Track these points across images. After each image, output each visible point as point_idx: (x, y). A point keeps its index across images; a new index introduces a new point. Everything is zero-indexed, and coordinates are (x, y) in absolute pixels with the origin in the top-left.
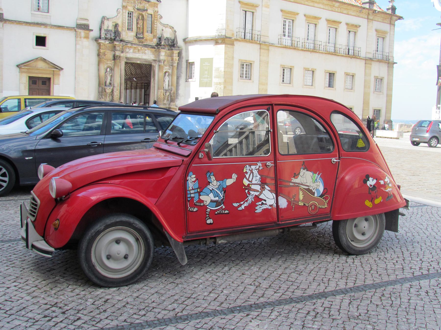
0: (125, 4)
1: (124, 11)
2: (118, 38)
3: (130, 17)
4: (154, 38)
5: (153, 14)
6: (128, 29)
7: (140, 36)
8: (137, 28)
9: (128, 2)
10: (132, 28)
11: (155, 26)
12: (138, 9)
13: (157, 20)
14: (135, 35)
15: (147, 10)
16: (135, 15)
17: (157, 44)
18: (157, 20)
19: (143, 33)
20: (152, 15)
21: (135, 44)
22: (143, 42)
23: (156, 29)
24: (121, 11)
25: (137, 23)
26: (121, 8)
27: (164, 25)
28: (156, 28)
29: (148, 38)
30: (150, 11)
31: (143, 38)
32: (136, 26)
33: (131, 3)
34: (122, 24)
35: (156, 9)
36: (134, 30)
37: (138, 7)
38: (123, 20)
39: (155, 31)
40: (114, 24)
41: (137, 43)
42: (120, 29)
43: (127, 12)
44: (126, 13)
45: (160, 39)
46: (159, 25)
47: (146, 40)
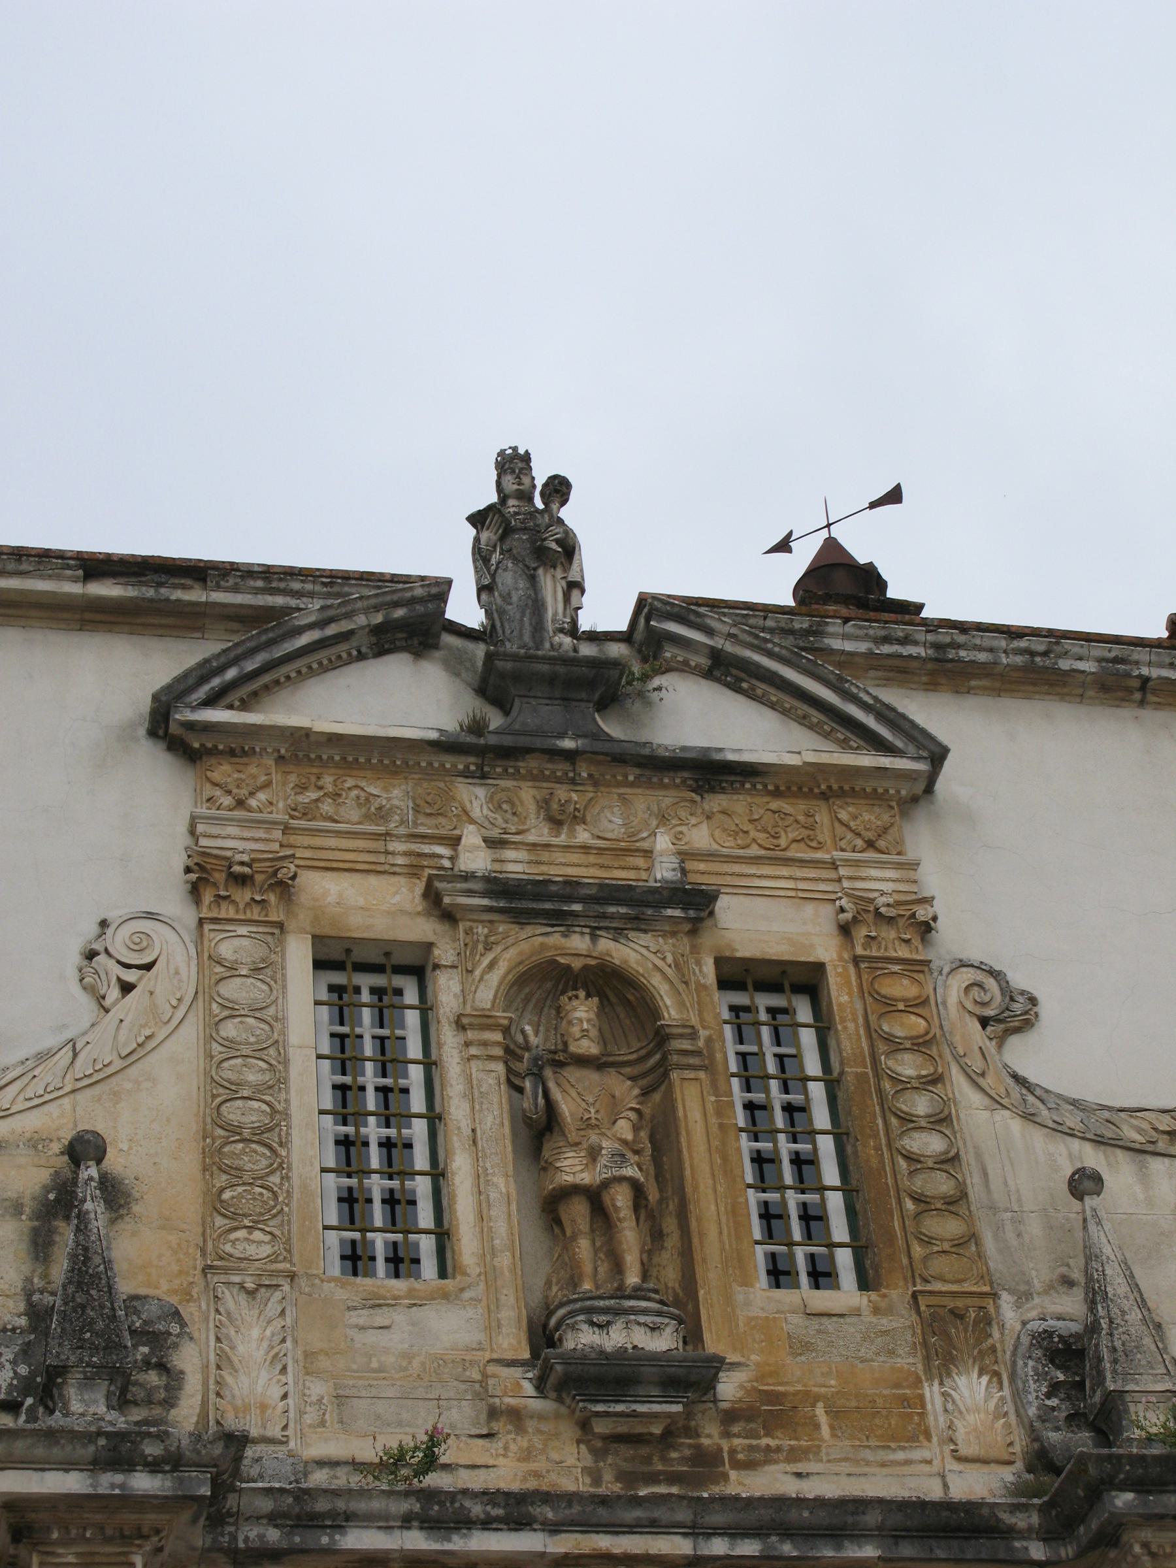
0: (235, 841)
1: (236, 945)
2: (86, 1405)
3: (389, 1059)
4: (941, 1358)
5: (824, 948)
6: (355, 1259)
7: (616, 1338)
8: (552, 1206)
9: (307, 813)
10: (443, 1235)
11: (931, 1144)
12: (518, 900)
13: (921, 1044)
14: (513, 1341)
15: (694, 903)
16: (472, 982)
17: (1042, 1460)
18: (921, 1044)
19: (686, 1313)
20: (806, 980)
21: (515, 1510)
22: (707, 1464)
23: (956, 1201)
24: (174, 950)
25: (539, 1132)
26: (175, 904)
27: (1103, 1127)
28: (940, 1185)
29: (796, 1375)
30: (766, 920)
31: (692, 1378)
32: (502, 1184)
33: (382, 814)
34: (213, 1161)
35: (881, 883)
36: (467, 1245)
37: (516, 865)
38: (221, 1091)
39: (947, 1227)
40: (29, 1178)
41: (573, 1482)
42: (145, 1257)
43: (298, 955)
44: (266, 969)
45: (1070, 1358)
46: (982, 1122)
47: (772, 1412)
